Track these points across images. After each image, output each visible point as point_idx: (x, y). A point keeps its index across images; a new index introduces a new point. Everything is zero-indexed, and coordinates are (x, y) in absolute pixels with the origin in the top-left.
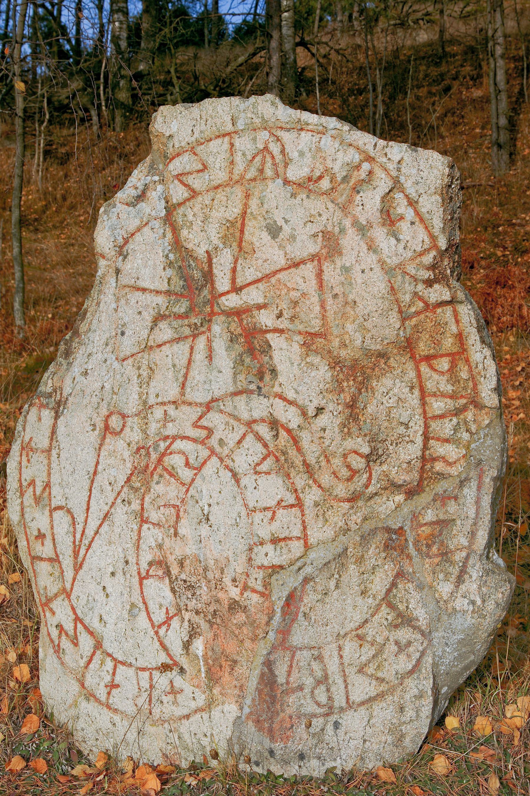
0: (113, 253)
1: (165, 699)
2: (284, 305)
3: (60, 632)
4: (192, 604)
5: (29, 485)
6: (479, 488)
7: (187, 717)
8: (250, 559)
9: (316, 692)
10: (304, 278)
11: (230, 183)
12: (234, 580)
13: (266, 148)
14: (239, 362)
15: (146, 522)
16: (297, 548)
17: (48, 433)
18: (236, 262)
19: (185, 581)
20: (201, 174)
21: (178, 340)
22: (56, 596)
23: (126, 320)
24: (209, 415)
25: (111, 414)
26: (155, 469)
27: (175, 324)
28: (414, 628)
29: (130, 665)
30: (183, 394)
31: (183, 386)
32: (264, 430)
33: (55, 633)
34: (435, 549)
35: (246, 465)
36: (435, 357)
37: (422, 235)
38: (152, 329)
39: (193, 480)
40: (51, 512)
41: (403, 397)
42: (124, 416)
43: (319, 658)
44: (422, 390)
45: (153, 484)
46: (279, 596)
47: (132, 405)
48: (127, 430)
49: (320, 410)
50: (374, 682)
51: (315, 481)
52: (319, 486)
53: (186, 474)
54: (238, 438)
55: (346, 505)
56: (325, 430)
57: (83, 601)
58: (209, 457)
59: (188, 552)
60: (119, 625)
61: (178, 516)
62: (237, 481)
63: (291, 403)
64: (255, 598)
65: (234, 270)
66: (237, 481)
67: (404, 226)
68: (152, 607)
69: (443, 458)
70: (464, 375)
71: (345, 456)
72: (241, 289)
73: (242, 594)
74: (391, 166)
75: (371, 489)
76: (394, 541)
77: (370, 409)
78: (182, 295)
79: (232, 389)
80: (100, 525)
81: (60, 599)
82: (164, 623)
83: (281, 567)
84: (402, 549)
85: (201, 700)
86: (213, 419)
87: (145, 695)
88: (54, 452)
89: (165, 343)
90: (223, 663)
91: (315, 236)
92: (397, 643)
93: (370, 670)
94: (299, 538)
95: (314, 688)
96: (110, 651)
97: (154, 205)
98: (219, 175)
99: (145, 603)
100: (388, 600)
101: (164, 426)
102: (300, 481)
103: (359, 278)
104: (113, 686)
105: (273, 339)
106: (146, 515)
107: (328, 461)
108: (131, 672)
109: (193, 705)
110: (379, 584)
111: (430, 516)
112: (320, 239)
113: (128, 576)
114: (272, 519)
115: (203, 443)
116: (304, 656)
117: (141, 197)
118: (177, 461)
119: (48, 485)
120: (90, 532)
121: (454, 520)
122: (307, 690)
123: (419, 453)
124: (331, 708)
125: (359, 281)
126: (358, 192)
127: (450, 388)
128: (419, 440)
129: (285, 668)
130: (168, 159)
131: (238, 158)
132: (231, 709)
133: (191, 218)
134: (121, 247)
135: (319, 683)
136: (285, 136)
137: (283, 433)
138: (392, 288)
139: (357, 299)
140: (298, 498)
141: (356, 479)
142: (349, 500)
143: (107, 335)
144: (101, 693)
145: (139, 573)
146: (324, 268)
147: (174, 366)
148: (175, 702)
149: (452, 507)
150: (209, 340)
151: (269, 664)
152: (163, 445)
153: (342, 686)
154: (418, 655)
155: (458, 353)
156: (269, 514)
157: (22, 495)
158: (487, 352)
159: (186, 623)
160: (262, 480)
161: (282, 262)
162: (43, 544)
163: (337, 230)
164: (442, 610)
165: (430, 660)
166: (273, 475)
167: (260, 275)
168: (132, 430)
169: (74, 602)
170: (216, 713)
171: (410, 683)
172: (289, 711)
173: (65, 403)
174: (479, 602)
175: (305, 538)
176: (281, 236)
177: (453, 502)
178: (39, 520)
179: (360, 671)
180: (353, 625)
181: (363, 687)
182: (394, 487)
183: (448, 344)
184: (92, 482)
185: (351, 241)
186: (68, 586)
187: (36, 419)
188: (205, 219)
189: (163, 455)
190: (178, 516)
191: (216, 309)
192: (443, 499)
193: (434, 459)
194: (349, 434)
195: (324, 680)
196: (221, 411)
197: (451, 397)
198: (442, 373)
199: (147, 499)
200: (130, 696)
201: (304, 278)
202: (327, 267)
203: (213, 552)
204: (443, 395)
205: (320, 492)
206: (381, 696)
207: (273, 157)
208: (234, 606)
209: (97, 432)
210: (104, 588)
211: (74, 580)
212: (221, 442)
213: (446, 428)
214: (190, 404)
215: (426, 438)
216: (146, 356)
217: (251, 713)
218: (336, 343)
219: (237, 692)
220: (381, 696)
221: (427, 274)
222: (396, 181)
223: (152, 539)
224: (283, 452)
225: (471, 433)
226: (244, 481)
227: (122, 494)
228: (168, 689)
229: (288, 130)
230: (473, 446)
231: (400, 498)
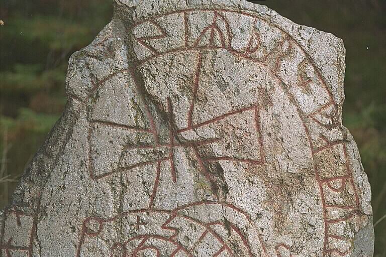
0: (85, 95)
13: (215, 25)
24: (176, 219)
27: (143, 151)
31: (153, 198)
32: (221, 229)
36: (331, 179)
41: (311, 206)
42: (101, 221)
44: (324, 203)
47: (111, 210)
49: (259, 215)
56: (262, 230)
65: (191, 113)
69: (337, 249)
70: (351, 191)
79: (193, 200)
86: (179, 221)
88: (36, 250)
89: (134, 166)
105: (226, 165)
107: (265, 251)
112: (257, 92)
115: (170, 239)
125: (285, 124)
131: (193, 30)
133: (154, 72)
137: (234, 232)
139: (284, 137)
146: (261, 114)
147: (144, 183)
152: (137, 242)
155: (346, 176)
185: (279, 94)
196: (185, 216)
197: (342, 207)
198: (336, 190)
202: (262, 113)
207: (220, 31)
212: (187, 238)
221: (328, 121)
225: (355, 233)
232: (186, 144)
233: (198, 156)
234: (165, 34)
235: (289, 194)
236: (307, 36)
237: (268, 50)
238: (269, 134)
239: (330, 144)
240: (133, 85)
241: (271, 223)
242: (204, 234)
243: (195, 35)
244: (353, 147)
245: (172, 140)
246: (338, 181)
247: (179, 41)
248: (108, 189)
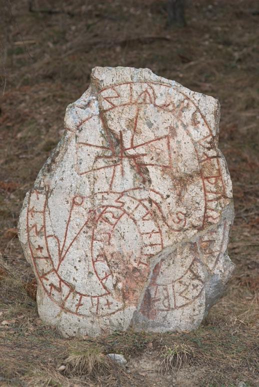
1: (104, 307)
6: (224, 229)
11: (131, 103)
15: (95, 240)
19: (114, 262)
20: (117, 99)
24: (123, 197)
26: (99, 219)
27: (106, 160)
32: (147, 203)
34: (207, 251)
35: (139, 217)
36: (209, 177)
39: (116, 223)
40: (46, 238)
41: (198, 192)
43: (166, 289)
45: (98, 225)
47: (87, 192)
50: (185, 299)
51: (166, 223)
54: (136, 206)
55: (177, 233)
56: (169, 204)
58: (123, 214)
59: (115, 250)
61: (110, 237)
63: (157, 193)
68: (99, 272)
70: (220, 185)
71: (177, 214)
72: (135, 147)
75: (186, 227)
76: (193, 247)
77: (186, 196)
79: (133, 187)
83: (153, 255)
86: (125, 199)
87: (96, 307)
88: (47, 213)
90: (130, 292)
91: (167, 128)
93: (184, 295)
95: (164, 300)
100: (190, 269)
102: (161, 223)
103: (183, 146)
104: (80, 305)
106: (95, 237)
107: (171, 216)
108: (89, 298)
110: (188, 261)
111: (206, 238)
113: (87, 261)
114: (150, 237)
116: (161, 288)
118: (109, 215)
119: (44, 227)
120: (67, 245)
121: (215, 241)
123: (203, 214)
124: (169, 308)
125: (184, 147)
126: (183, 112)
127: (215, 190)
128: (203, 209)
129: (154, 292)
131: (134, 94)
135: (165, 298)
137: (154, 205)
138: (196, 150)
141: (181, 223)
145: (93, 260)
148: (109, 308)
149: (214, 235)
150: (122, 168)
152: (102, 209)
153: (174, 300)
154: (200, 290)
159: (115, 278)
161: (153, 138)
167: (144, 142)
168: (87, 203)
172: (155, 308)
174: (223, 271)
175: (162, 244)
176: (153, 127)
177: (215, 233)
179: (180, 295)
180: (178, 277)
182: (194, 227)
183: (215, 172)
186: (56, 268)
187: (36, 199)
189: (102, 213)
190: (110, 237)
195: (167, 297)
197: (215, 193)
199: (95, 231)
200: (88, 308)
201: (162, 145)
202: (171, 140)
203: (126, 250)
204: (212, 192)
205: (167, 227)
208: (135, 270)
209: (69, 205)
211: (59, 265)
212: (129, 208)
215: (206, 209)
216: (92, 173)
217: (141, 309)
218: (174, 170)
220: (187, 304)
221: (208, 145)
223: (98, 246)
225: (222, 208)
226: (139, 223)
227: (83, 229)
231: (196, 231)
236: (198, 99)
237: (176, 106)
243: (135, 97)
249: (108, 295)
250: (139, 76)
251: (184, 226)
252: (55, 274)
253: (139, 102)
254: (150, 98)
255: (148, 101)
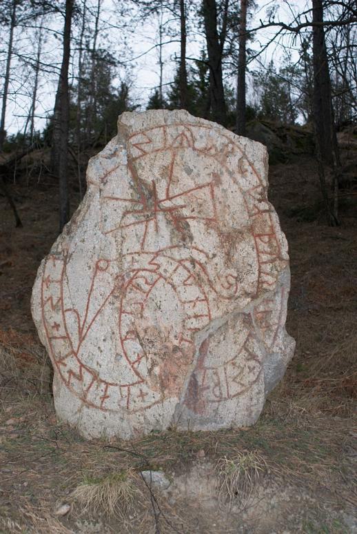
1: (137, 400)
2: (194, 206)
3: (70, 375)
4: (153, 350)
5: (48, 300)
7: (150, 407)
8: (184, 326)
9: (215, 390)
10: (204, 194)
11: (165, 148)
12: (176, 337)
13: (183, 134)
14: (172, 233)
16: (206, 320)
17: (60, 272)
18: (169, 185)
21: (138, 223)
22: (67, 356)
23: (107, 213)
25: (100, 261)
27: (136, 215)
28: (256, 360)
29: (116, 385)
30: (142, 248)
31: (142, 245)
32: (188, 264)
33: (66, 376)
34: (264, 324)
36: (262, 235)
37: (256, 179)
38: (123, 218)
39: (150, 290)
43: (216, 373)
44: (257, 250)
46: (198, 344)
47: (113, 254)
48: (110, 267)
52: (215, 291)
53: (147, 288)
54: (174, 268)
55: (227, 301)
56: (217, 264)
57: (86, 356)
59: (149, 324)
60: (109, 365)
61: (142, 308)
62: (175, 289)
63: (201, 251)
64: (187, 344)
65: (168, 190)
66: (175, 289)
67: (248, 174)
68: (129, 353)
70: (275, 245)
71: (226, 277)
72: (172, 198)
73: (180, 343)
74: (242, 147)
75: (237, 294)
76: (247, 320)
78: (139, 202)
79: (170, 245)
80: (96, 317)
81: (69, 358)
82: (136, 361)
83: (199, 329)
84: (250, 323)
85: (158, 396)
86: (161, 260)
87: (126, 399)
88: (65, 282)
89: (130, 225)
90: (170, 378)
91: (209, 174)
92: (249, 367)
93: (238, 380)
94: (207, 316)
96: (103, 379)
97: (122, 159)
98: (159, 145)
99: (125, 354)
100: (245, 347)
101: (132, 265)
102: (207, 289)
103: (231, 196)
104: (105, 397)
105: (191, 222)
108: (117, 388)
109: (153, 400)
110: (242, 338)
111: (262, 308)
115: (155, 271)
116: (210, 372)
117: (114, 154)
118: (141, 281)
119: (61, 299)
120: (89, 320)
122: (211, 389)
125: (231, 196)
128: (257, 273)
129: (202, 377)
130: (128, 137)
132: (175, 400)
133: (143, 164)
134: (102, 179)
135: (216, 385)
136: (193, 129)
137: (197, 266)
138: (245, 201)
140: (206, 297)
142: (228, 299)
143: (96, 221)
144: (98, 402)
145: (121, 338)
146: (214, 189)
147: (137, 235)
149: (271, 305)
150: (156, 223)
151: (194, 376)
152: (132, 274)
153: (226, 387)
155: (272, 235)
156: (193, 304)
157: (43, 306)
158: (284, 235)
159: (150, 360)
160: (188, 288)
161: (193, 186)
162: (58, 330)
163: (219, 173)
164: (269, 353)
165: (263, 376)
166: (193, 286)
167: (182, 192)
169: (80, 357)
170: (166, 403)
171: (255, 386)
172: (203, 399)
173: (71, 256)
174: (283, 349)
178: (58, 318)
179: (234, 380)
180: (231, 358)
181: (235, 388)
182: (247, 294)
183: (267, 230)
184: (90, 295)
185: (225, 178)
186: (75, 349)
188: (152, 166)
189: (132, 279)
190: (142, 308)
191: (158, 208)
192: (267, 301)
193: (263, 282)
194: (228, 267)
195: (218, 384)
196: (164, 256)
198: (266, 243)
199: (124, 301)
200: (116, 401)
201: (204, 194)
202: (216, 189)
206: (242, 392)
207: (187, 138)
208: (176, 349)
209: (91, 270)
210: (99, 348)
211: (79, 346)
212: (165, 271)
213: (268, 268)
214: (147, 253)
215: (260, 273)
217: (185, 401)
218: (221, 224)
219: (177, 391)
220: (242, 392)
221: (259, 197)
222: (244, 153)
224: (198, 275)
228: (139, 393)
229: (194, 126)
230: (279, 277)
231: (249, 299)
232: (165, 210)
233: (173, 217)
234: (150, 141)
235: (234, 243)
236: (244, 143)
237: (219, 150)
238: (220, 202)
239: (261, 212)
240: (130, 173)
241: (223, 261)
242: (177, 268)
243: (170, 141)
244: (275, 216)
245: (155, 208)
246: (266, 237)
247: (159, 145)
248: (113, 240)
249: (142, 384)
250: (174, 118)
251: (235, 292)
252: (75, 357)
253: (175, 146)
254: (188, 141)
255: (185, 144)
